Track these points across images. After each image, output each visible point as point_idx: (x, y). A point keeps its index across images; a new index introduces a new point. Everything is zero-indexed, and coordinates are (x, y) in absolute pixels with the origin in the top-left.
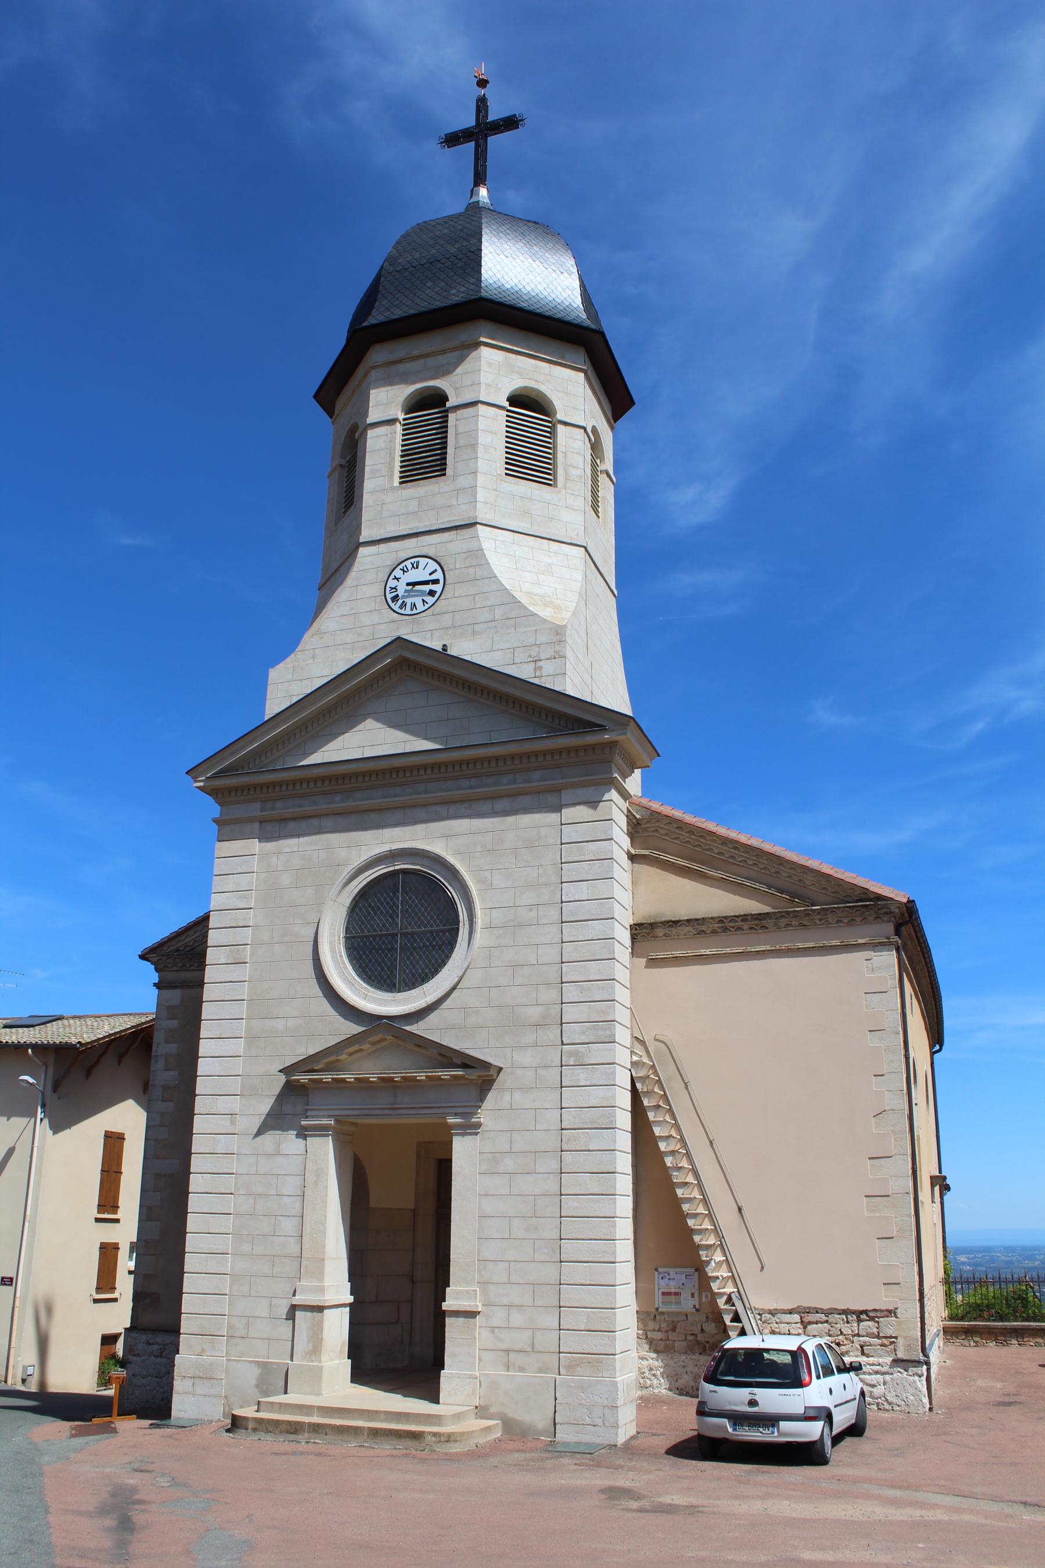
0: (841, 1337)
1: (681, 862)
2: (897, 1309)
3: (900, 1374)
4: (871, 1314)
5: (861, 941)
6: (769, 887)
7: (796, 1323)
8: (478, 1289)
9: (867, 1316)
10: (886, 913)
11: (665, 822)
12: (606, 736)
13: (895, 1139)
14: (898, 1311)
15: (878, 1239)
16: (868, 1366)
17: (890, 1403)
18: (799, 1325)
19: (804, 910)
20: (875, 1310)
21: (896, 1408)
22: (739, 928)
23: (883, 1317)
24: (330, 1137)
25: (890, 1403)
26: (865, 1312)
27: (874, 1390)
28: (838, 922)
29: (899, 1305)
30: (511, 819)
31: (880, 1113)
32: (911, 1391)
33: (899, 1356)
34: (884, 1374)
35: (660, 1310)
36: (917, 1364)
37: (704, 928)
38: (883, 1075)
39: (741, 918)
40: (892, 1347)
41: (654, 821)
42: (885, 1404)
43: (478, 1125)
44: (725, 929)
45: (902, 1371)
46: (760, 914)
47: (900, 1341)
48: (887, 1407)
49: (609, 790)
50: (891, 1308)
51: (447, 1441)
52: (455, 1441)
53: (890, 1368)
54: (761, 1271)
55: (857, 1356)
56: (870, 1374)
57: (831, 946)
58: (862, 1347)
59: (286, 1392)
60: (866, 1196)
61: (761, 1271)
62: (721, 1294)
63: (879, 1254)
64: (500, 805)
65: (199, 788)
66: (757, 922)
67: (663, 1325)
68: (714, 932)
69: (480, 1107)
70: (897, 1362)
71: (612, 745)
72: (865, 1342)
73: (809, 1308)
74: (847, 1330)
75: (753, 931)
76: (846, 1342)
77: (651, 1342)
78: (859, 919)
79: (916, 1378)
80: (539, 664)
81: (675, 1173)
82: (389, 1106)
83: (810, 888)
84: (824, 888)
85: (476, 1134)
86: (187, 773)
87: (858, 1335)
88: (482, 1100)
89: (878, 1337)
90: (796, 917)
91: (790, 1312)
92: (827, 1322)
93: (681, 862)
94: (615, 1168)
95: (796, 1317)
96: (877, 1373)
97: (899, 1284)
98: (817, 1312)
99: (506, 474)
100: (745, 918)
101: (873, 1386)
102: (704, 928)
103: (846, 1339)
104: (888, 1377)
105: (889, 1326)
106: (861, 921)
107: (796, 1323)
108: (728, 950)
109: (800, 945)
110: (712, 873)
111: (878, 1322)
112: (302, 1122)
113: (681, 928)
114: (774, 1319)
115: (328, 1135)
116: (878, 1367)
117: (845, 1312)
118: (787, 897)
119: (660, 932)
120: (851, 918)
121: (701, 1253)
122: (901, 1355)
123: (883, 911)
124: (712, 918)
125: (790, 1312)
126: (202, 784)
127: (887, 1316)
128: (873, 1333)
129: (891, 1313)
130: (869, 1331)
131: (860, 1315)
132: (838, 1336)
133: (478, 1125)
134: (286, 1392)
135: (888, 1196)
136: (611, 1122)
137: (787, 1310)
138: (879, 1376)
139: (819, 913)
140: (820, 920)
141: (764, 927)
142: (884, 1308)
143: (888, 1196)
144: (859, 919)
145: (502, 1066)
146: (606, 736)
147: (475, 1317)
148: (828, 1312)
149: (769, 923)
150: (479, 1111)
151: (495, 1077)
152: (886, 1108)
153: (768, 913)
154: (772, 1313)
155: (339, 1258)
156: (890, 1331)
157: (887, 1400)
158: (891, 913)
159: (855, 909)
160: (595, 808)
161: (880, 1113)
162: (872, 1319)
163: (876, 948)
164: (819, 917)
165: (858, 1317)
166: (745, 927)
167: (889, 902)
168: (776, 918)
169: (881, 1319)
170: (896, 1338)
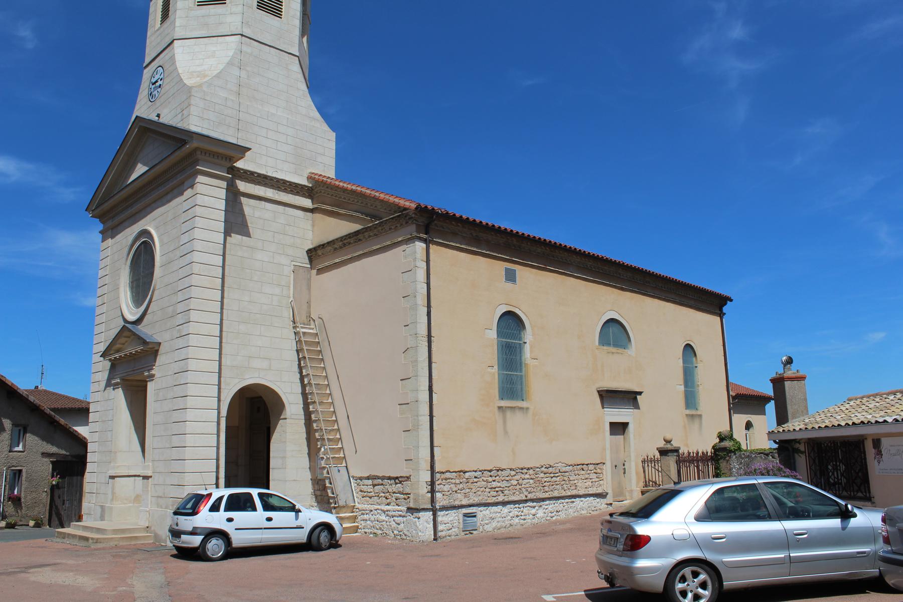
0: (388, 494)
1: (329, 208)
2: (410, 476)
3: (410, 517)
4: (400, 479)
5: (400, 239)
6: (362, 214)
7: (371, 485)
8: (151, 464)
9: (399, 480)
10: (410, 219)
11: (322, 185)
12: (188, 146)
13: (413, 367)
14: (411, 477)
15: (404, 431)
16: (397, 512)
17: (405, 535)
18: (371, 487)
19: (373, 225)
20: (401, 477)
21: (408, 538)
22: (350, 243)
23: (405, 481)
24: (120, 388)
25: (405, 535)
26: (397, 478)
27: (399, 526)
28: (390, 229)
29: (411, 474)
30: (171, 203)
31: (406, 350)
32: (414, 527)
33: (411, 506)
34: (404, 516)
35: (318, 478)
36: (416, 511)
37: (336, 246)
38: (408, 325)
39: (348, 236)
40: (408, 500)
41: (318, 186)
42: (404, 535)
43: (153, 376)
44: (344, 245)
45: (411, 515)
46: (355, 232)
47: (411, 496)
48: (404, 537)
49: (197, 177)
50: (408, 475)
51: (96, 542)
52: (101, 542)
53: (406, 513)
54: (356, 453)
55: (394, 506)
56: (398, 517)
57: (387, 246)
58: (396, 499)
59: (102, 518)
60: (399, 404)
61: (356, 453)
62: (324, 468)
63: (404, 441)
64: (169, 196)
65: (91, 217)
66: (355, 238)
67: (320, 487)
68: (341, 248)
69: (154, 365)
70: (410, 510)
71: (196, 150)
72: (397, 497)
73: (374, 476)
74: (390, 490)
75: (356, 243)
76: (389, 497)
77: (316, 497)
78: (398, 225)
79: (417, 519)
80: (183, 112)
81: (310, 397)
82: (131, 370)
83: (381, 210)
84: (385, 209)
85: (153, 380)
86: (86, 210)
87: (394, 493)
88: (155, 362)
89: (403, 494)
90: (371, 230)
91: (368, 478)
92: (382, 484)
93: (329, 208)
94: (187, 393)
95: (370, 482)
96: (400, 516)
97: (412, 460)
98: (379, 479)
99: (257, 8)
100: (349, 236)
101: (399, 524)
102: (336, 246)
103: (390, 495)
104: (405, 519)
105: (407, 487)
106: (400, 226)
107: (371, 485)
108: (345, 258)
109: (375, 248)
110: (342, 211)
111: (402, 484)
112: (113, 382)
113: (326, 248)
114: (361, 483)
115: (118, 388)
116: (401, 512)
117: (390, 478)
118: (369, 218)
119: (320, 252)
120: (395, 226)
121: (318, 443)
122: (412, 505)
123: (408, 217)
124: (337, 239)
125: (368, 478)
126: (91, 215)
127: (407, 481)
128: (400, 492)
129: (408, 478)
130: (399, 490)
131: (397, 479)
132: (387, 493)
133: (153, 376)
134: (102, 520)
135: (408, 404)
136: (187, 368)
137: (366, 477)
138: (401, 518)
139: (380, 226)
140: (382, 229)
141: (360, 240)
142: (405, 476)
143: (408, 404)
144: (398, 225)
145: (160, 341)
146: (188, 146)
147: (148, 479)
148: (383, 478)
149: (360, 236)
150: (154, 367)
151: (156, 348)
152: (409, 346)
153: (358, 231)
154: (361, 479)
155: (132, 451)
156: (407, 490)
157: (404, 533)
158: (412, 218)
159: (395, 219)
160: (192, 188)
161: (406, 350)
162: (400, 482)
163: (408, 242)
164: (380, 228)
165: (395, 481)
166: (352, 242)
167: (408, 211)
168: (363, 233)
169: (404, 482)
170: (410, 494)
